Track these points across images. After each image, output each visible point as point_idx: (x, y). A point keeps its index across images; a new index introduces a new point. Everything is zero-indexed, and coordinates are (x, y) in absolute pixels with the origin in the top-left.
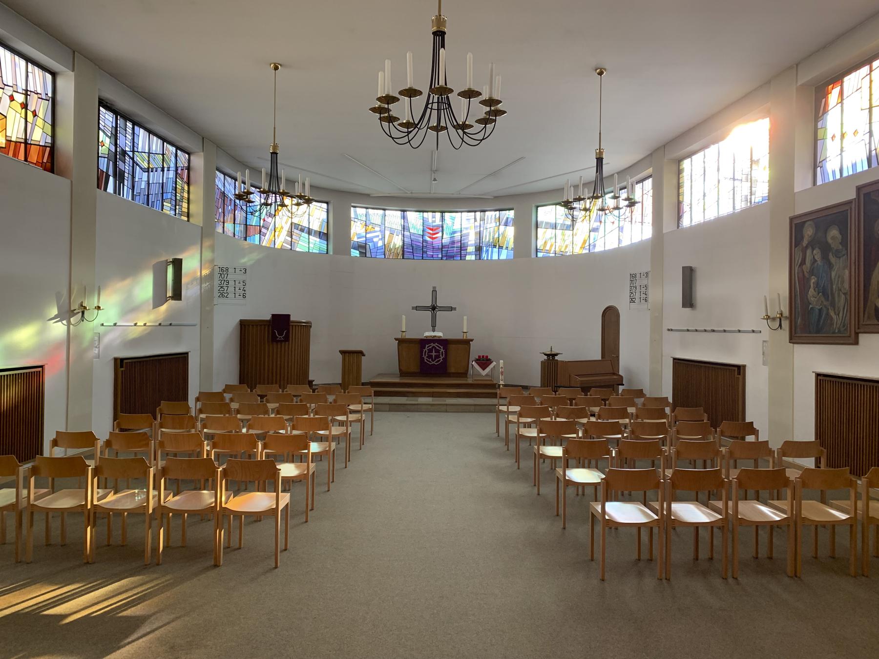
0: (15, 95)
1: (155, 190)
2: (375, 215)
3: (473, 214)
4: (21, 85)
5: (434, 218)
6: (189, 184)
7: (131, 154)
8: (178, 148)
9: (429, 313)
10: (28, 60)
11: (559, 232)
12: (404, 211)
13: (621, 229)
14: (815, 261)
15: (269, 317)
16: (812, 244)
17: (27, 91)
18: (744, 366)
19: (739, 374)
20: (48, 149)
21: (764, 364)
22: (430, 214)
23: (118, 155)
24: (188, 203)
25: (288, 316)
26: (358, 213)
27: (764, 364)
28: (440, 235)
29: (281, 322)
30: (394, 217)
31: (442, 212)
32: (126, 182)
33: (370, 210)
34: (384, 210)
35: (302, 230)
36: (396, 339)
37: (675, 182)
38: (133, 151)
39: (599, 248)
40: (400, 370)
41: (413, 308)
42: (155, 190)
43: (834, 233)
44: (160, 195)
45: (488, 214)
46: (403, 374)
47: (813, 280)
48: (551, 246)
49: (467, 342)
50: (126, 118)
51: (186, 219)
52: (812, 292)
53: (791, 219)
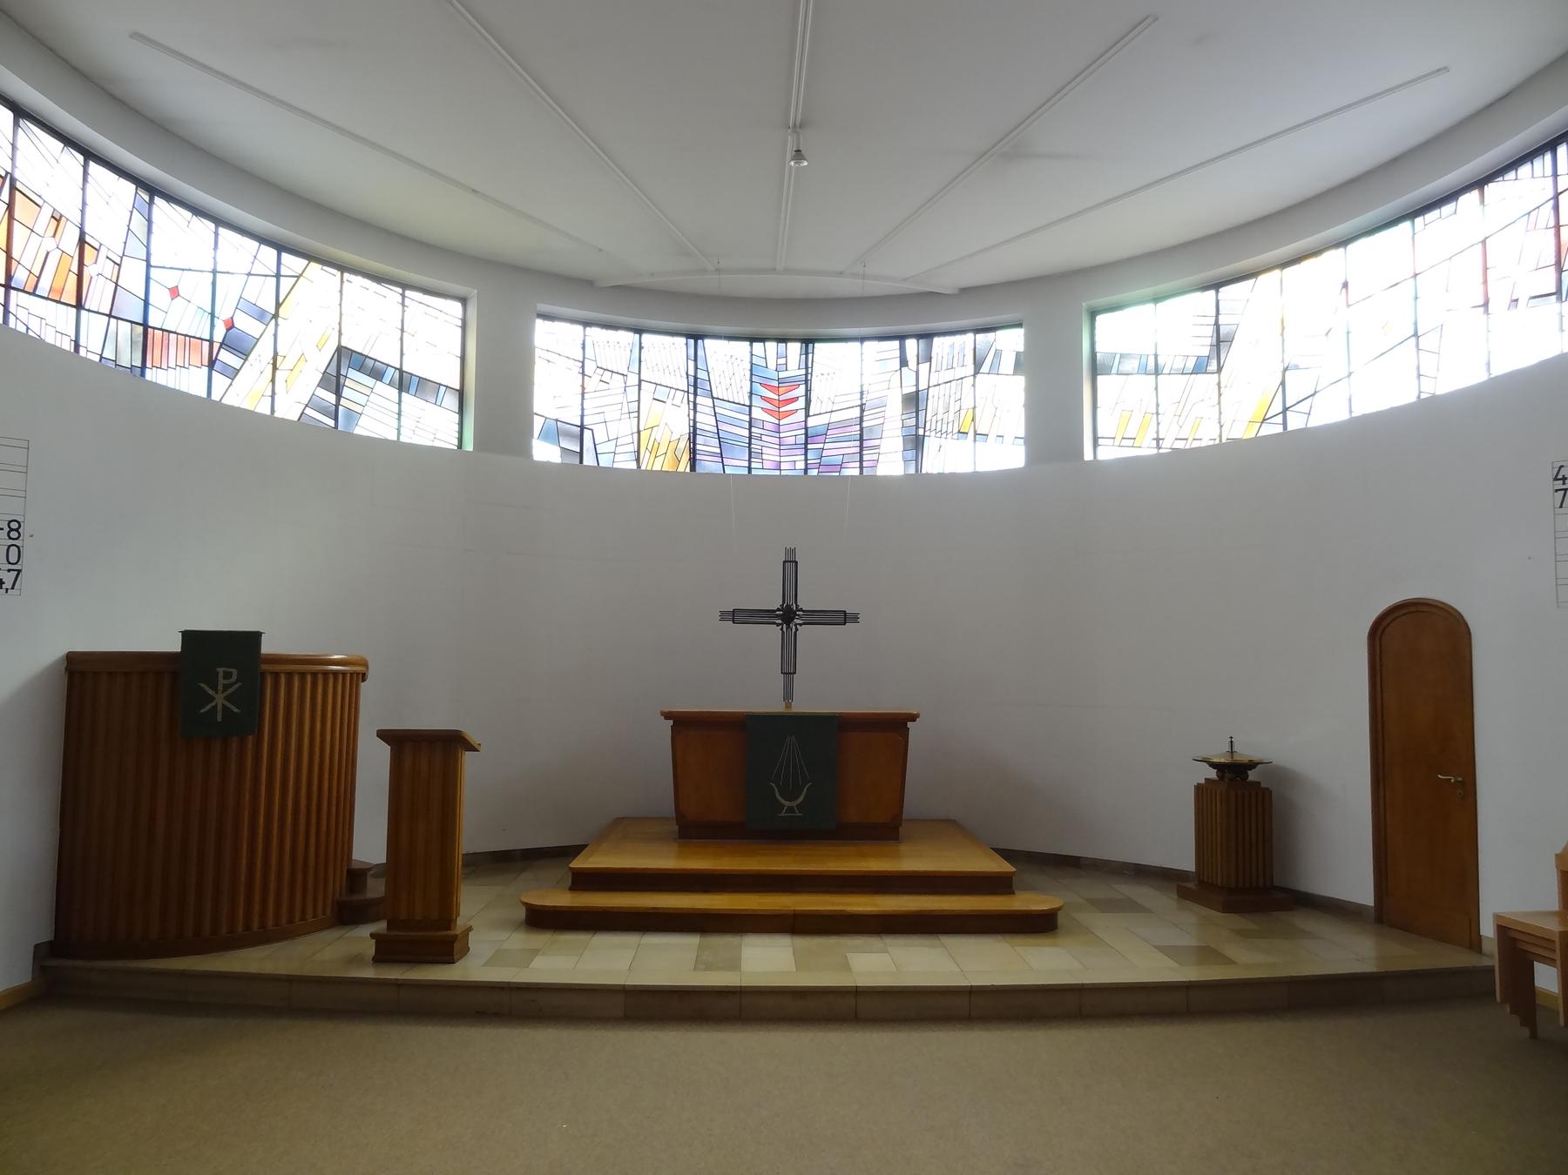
2: (613, 345)
3: (896, 344)
9: (773, 633)
12: (696, 337)
22: (771, 346)
25: (254, 638)
28: (801, 403)
29: (220, 655)
30: (666, 354)
31: (808, 341)
33: (594, 332)
34: (639, 331)
35: (377, 374)
36: (667, 716)
40: (680, 816)
41: (724, 616)
49: (896, 726)
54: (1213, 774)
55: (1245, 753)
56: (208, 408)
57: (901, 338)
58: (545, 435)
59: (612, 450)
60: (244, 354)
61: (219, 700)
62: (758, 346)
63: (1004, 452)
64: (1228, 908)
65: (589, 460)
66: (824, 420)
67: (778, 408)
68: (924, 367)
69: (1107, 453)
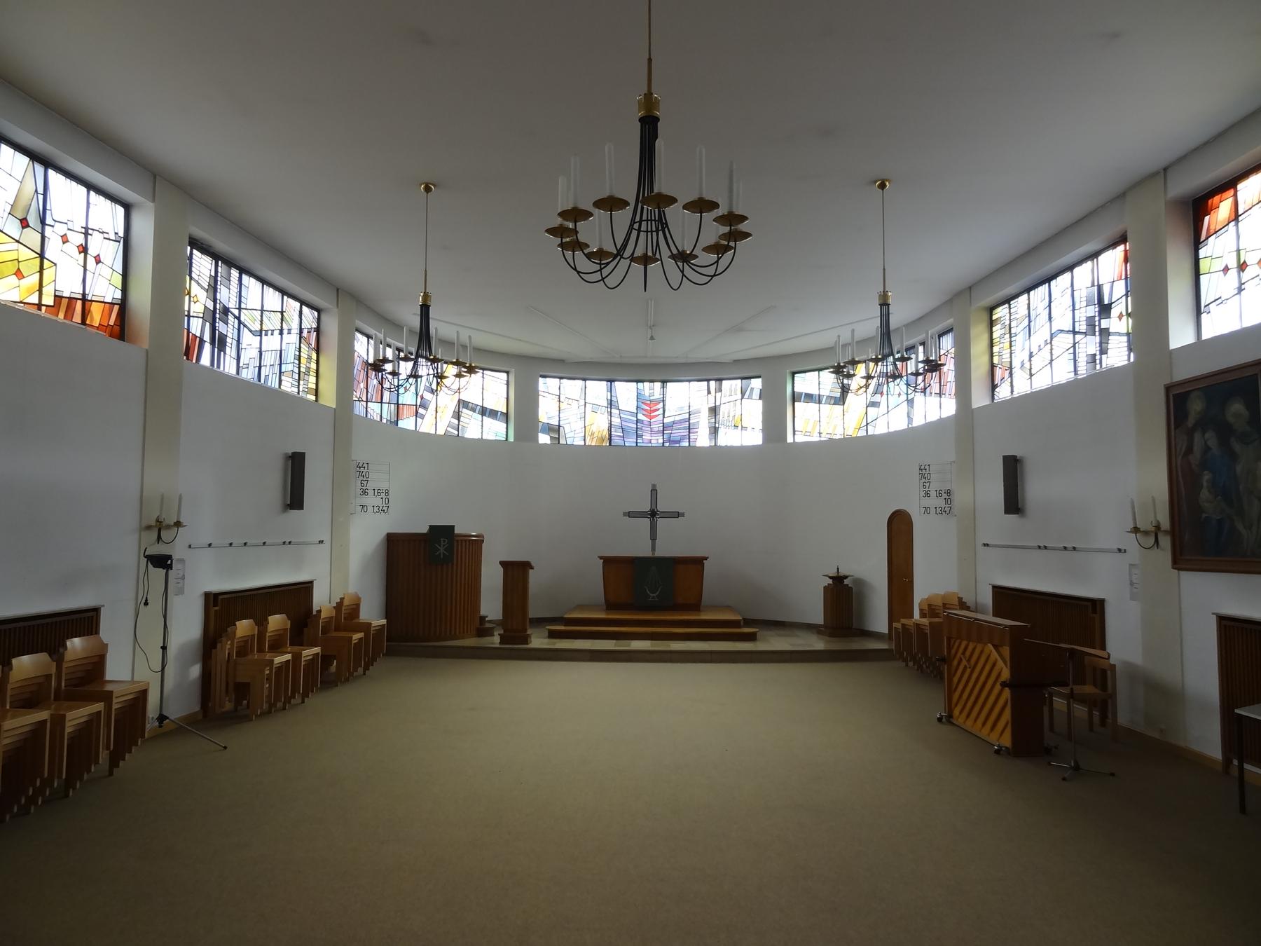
0: (70, 235)
1: (269, 359)
2: (572, 387)
4: (79, 224)
5: (652, 390)
6: (318, 351)
7: (236, 312)
8: (303, 303)
10: (90, 186)
11: (826, 408)
13: (910, 402)
14: (1207, 449)
15: (425, 530)
16: (1202, 424)
17: (86, 229)
18: (1102, 602)
19: (1094, 611)
20: (116, 307)
21: (1133, 598)
22: (647, 384)
23: (217, 314)
24: (317, 377)
26: (547, 386)
27: (1133, 598)
28: (661, 411)
29: (442, 533)
30: (597, 390)
31: (664, 382)
32: (228, 350)
34: (585, 380)
35: (473, 410)
36: (601, 558)
37: (986, 336)
38: (240, 309)
39: (879, 429)
41: (625, 514)
42: (269, 359)
43: (1236, 409)
44: (277, 368)
45: (726, 384)
46: (610, 606)
47: (1207, 477)
48: (814, 427)
49: (699, 562)
50: (230, 263)
51: (313, 398)
52: (1205, 494)
53: (1168, 389)
54: (830, 581)
55: (843, 572)
56: (416, 433)
57: (708, 380)
58: (543, 432)
59: (573, 435)
60: (426, 408)
61: (442, 550)
62: (640, 385)
63: (754, 437)
64: (831, 635)
65: (562, 441)
66: (671, 419)
67: (650, 414)
68: (718, 395)
69: (800, 439)
